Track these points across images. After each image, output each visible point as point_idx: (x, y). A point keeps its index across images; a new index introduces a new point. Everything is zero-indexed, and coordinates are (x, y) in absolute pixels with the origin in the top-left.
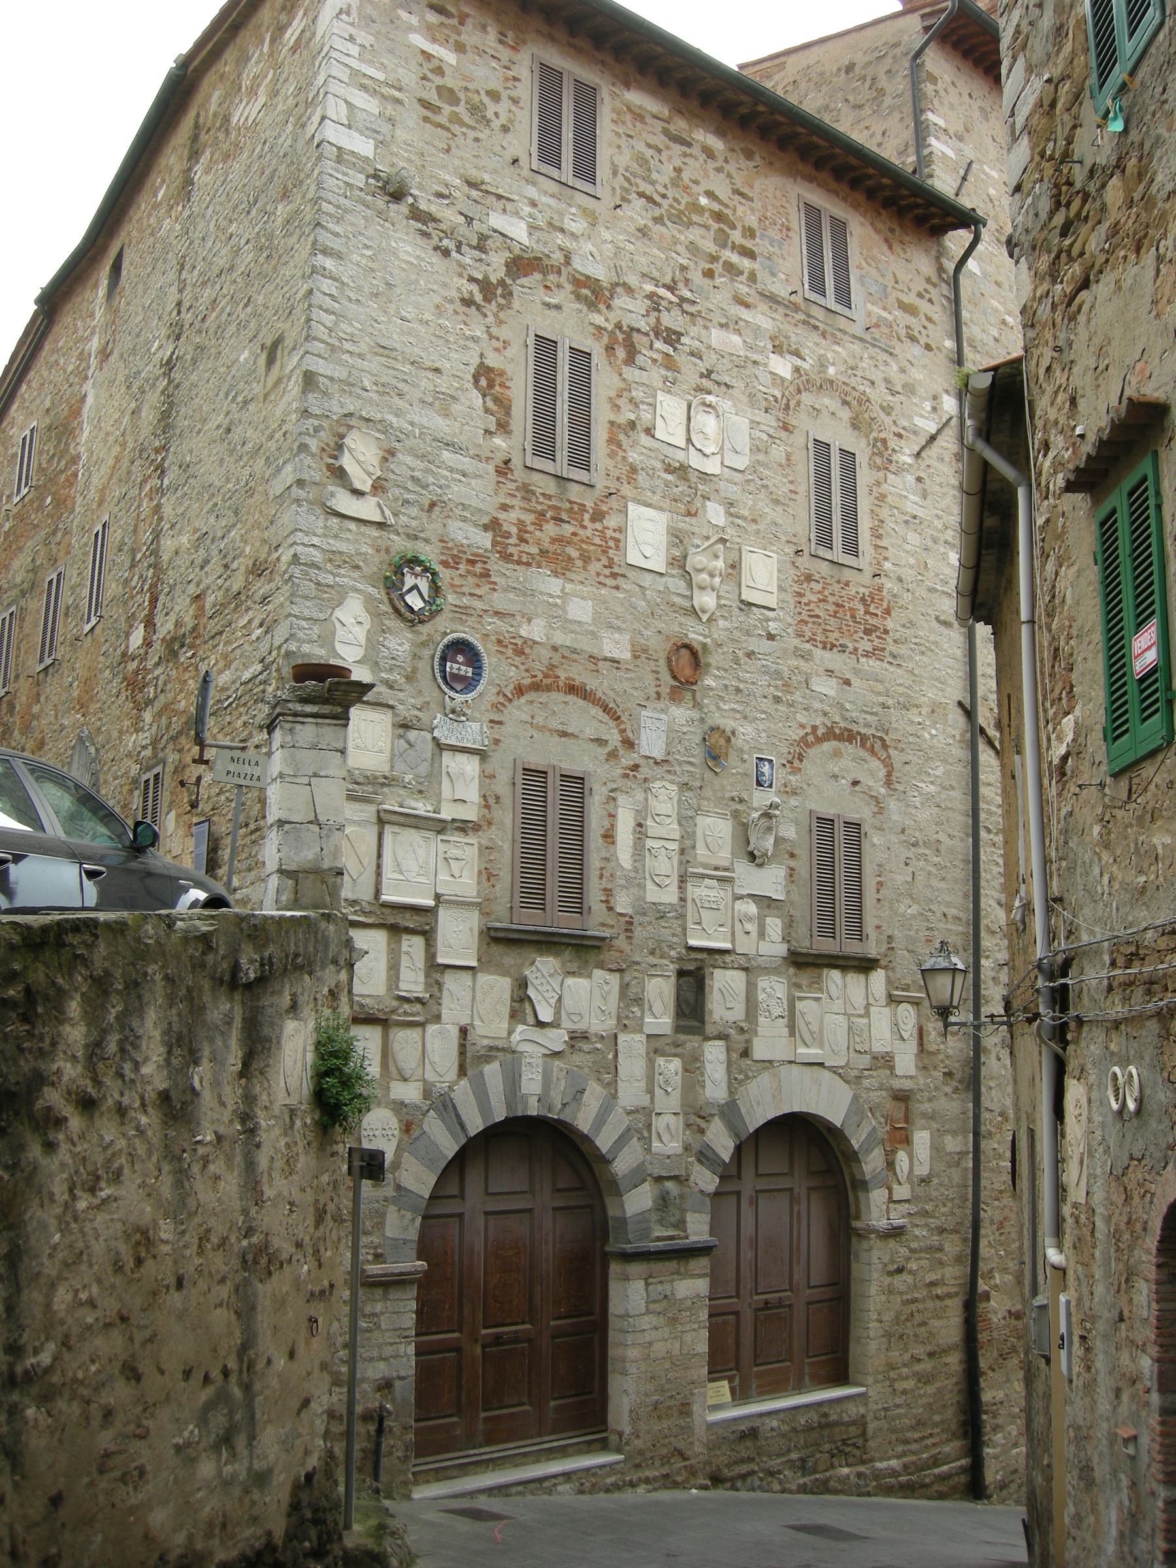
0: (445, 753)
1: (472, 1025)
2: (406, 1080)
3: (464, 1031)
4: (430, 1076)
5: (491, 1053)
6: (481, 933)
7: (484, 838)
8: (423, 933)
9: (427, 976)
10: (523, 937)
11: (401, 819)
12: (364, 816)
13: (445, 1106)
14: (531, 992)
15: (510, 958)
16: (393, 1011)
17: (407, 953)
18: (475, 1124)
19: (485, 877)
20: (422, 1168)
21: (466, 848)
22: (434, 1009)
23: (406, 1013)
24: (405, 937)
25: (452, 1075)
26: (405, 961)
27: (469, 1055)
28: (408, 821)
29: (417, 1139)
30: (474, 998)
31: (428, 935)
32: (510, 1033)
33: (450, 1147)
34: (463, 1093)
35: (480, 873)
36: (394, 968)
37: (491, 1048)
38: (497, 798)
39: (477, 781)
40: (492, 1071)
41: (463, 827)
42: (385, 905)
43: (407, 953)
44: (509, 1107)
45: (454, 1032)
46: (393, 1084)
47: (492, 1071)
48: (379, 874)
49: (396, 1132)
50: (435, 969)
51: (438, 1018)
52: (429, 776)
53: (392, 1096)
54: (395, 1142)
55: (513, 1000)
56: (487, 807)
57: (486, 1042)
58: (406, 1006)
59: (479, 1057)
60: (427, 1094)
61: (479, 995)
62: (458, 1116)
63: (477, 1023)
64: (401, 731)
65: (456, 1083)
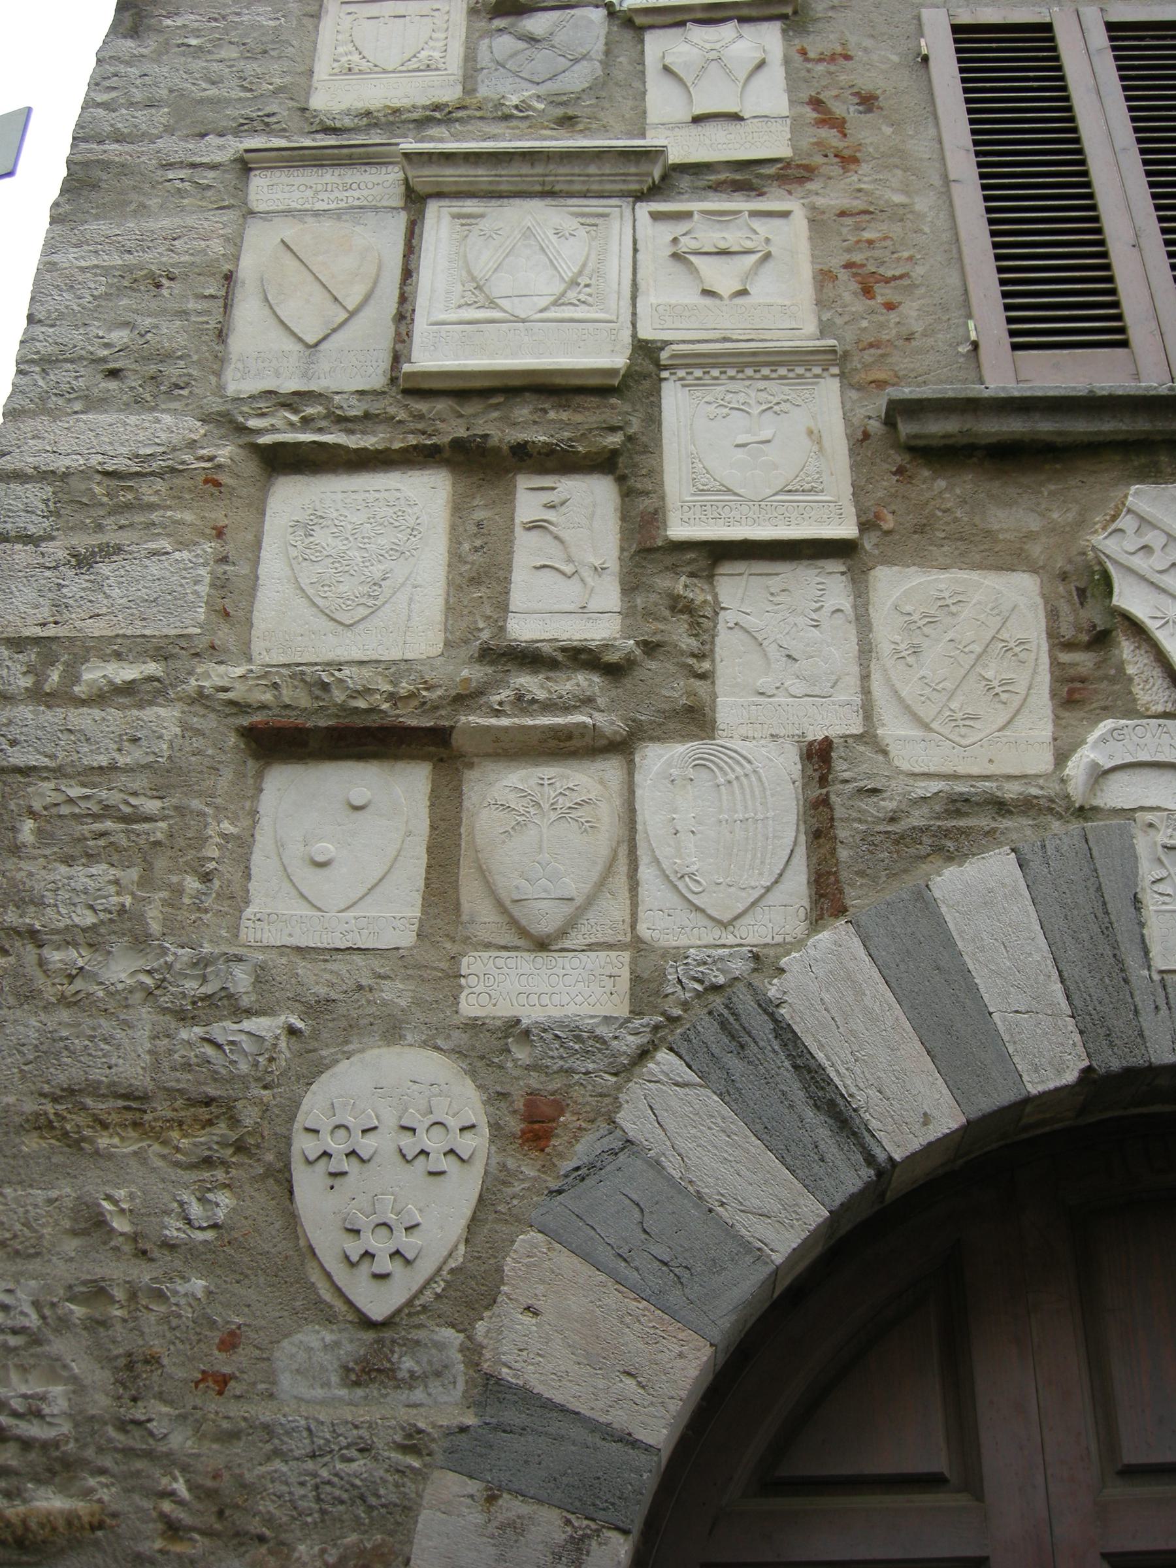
0: (650, 37)
1: (868, 737)
2: (542, 945)
3: (819, 756)
4: (663, 924)
5: (966, 816)
6: (860, 441)
7: (833, 195)
8: (603, 463)
9: (630, 587)
10: (1045, 426)
11: (482, 175)
12: (354, 197)
13: (732, 1029)
14: (1130, 598)
15: (1019, 511)
16: (464, 699)
17: (535, 526)
18: (914, 1108)
19: (847, 288)
20: (613, 1297)
21: (756, 224)
22: (676, 690)
23: (522, 703)
24: (524, 482)
25: (783, 914)
26: (527, 551)
27: (842, 834)
28: (507, 175)
29: (580, 1174)
30: (866, 651)
31: (625, 463)
32: (1061, 758)
33: (777, 1211)
34: (834, 988)
35: (824, 277)
36: (480, 574)
37: (958, 805)
38: (867, 101)
39: (776, 73)
40: (984, 897)
41: (744, 177)
42: (421, 389)
43: (535, 526)
44: (1089, 1022)
45: (783, 767)
46: (473, 963)
47: (984, 897)
48: (403, 317)
49: (476, 1144)
50: (650, 551)
51: (695, 720)
52: (599, 88)
53: (470, 1006)
54: (461, 1192)
55: (1060, 643)
56: (839, 125)
57: (935, 786)
58: (530, 683)
59: (899, 840)
60: (645, 990)
61: (886, 633)
62: (810, 1073)
63: (893, 729)
64: (499, 23)
65: (799, 944)
